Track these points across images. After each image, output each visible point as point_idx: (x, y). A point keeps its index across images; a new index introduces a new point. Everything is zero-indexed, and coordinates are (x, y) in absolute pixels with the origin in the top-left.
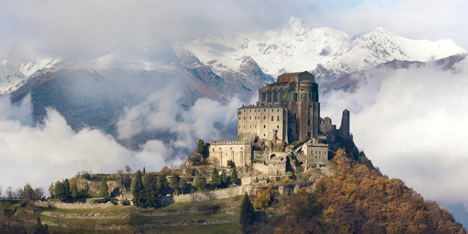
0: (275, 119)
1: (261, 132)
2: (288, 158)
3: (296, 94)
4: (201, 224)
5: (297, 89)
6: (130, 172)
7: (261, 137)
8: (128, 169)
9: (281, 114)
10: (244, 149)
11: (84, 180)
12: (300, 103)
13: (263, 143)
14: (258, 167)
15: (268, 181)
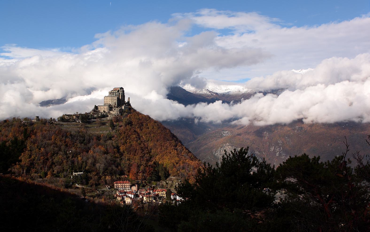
0: (115, 100)
1: (111, 103)
2: (119, 110)
3: (119, 93)
4: (99, 127)
5: (120, 92)
6: (78, 114)
7: (111, 104)
8: (77, 113)
9: (116, 98)
10: (107, 107)
11: (66, 116)
12: (120, 95)
13: (112, 106)
14: (111, 112)
15: (115, 116)
